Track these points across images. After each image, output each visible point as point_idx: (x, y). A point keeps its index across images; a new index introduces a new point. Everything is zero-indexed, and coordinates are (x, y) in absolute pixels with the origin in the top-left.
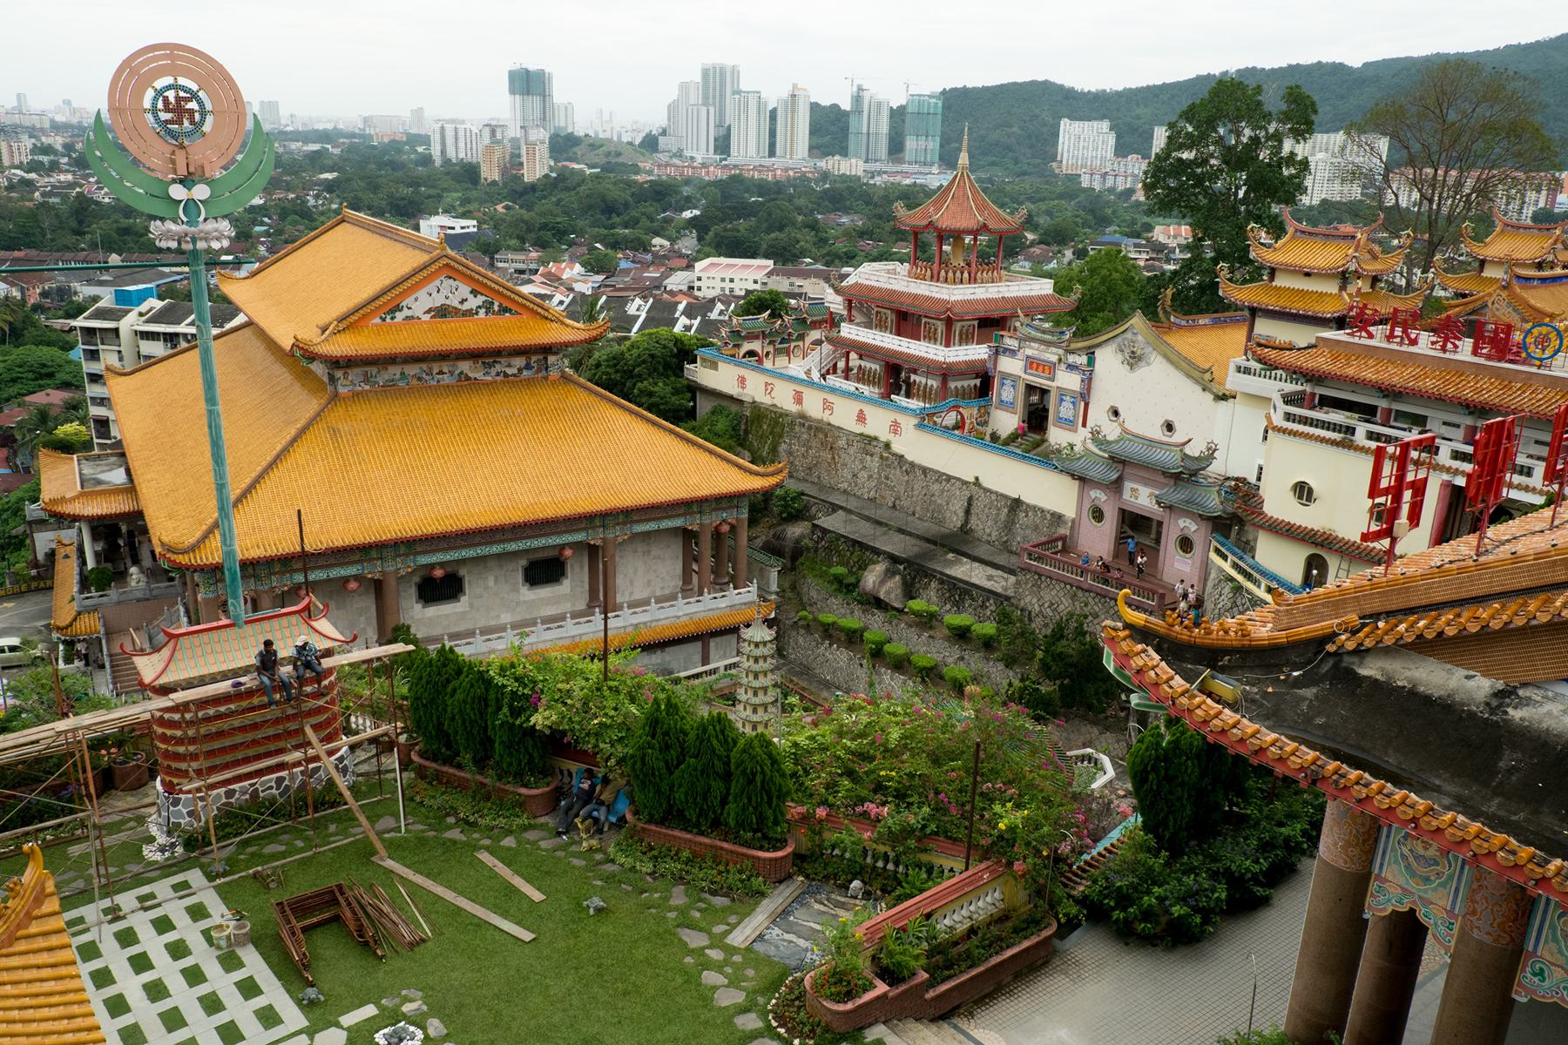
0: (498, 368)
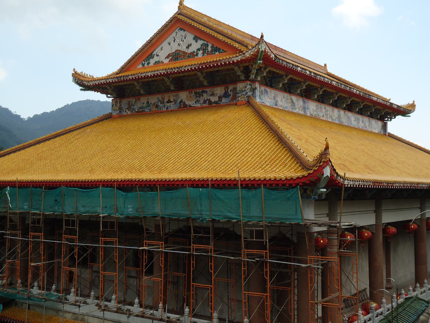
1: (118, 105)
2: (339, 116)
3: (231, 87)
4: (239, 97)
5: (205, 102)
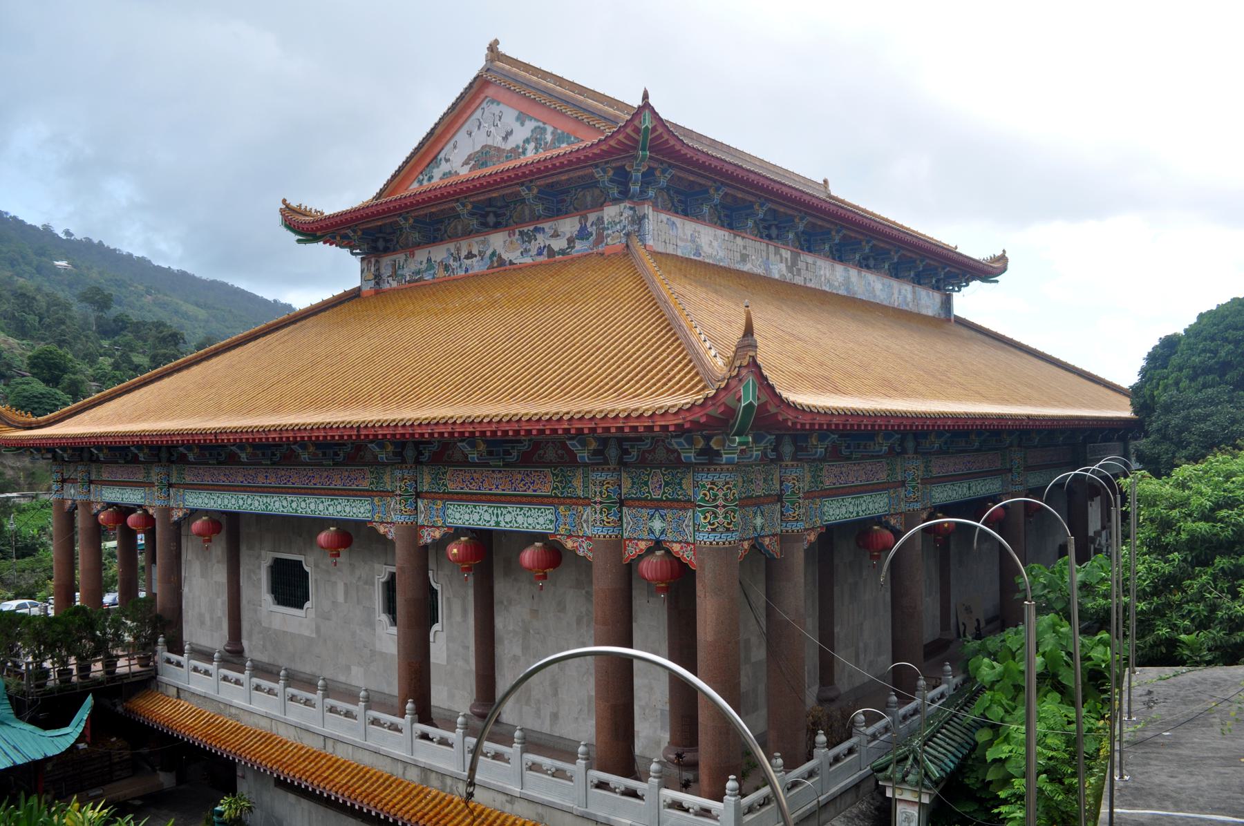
0: (541, 240)
1: (373, 269)
2: (847, 279)
3: (592, 217)
4: (608, 235)
5: (540, 254)
